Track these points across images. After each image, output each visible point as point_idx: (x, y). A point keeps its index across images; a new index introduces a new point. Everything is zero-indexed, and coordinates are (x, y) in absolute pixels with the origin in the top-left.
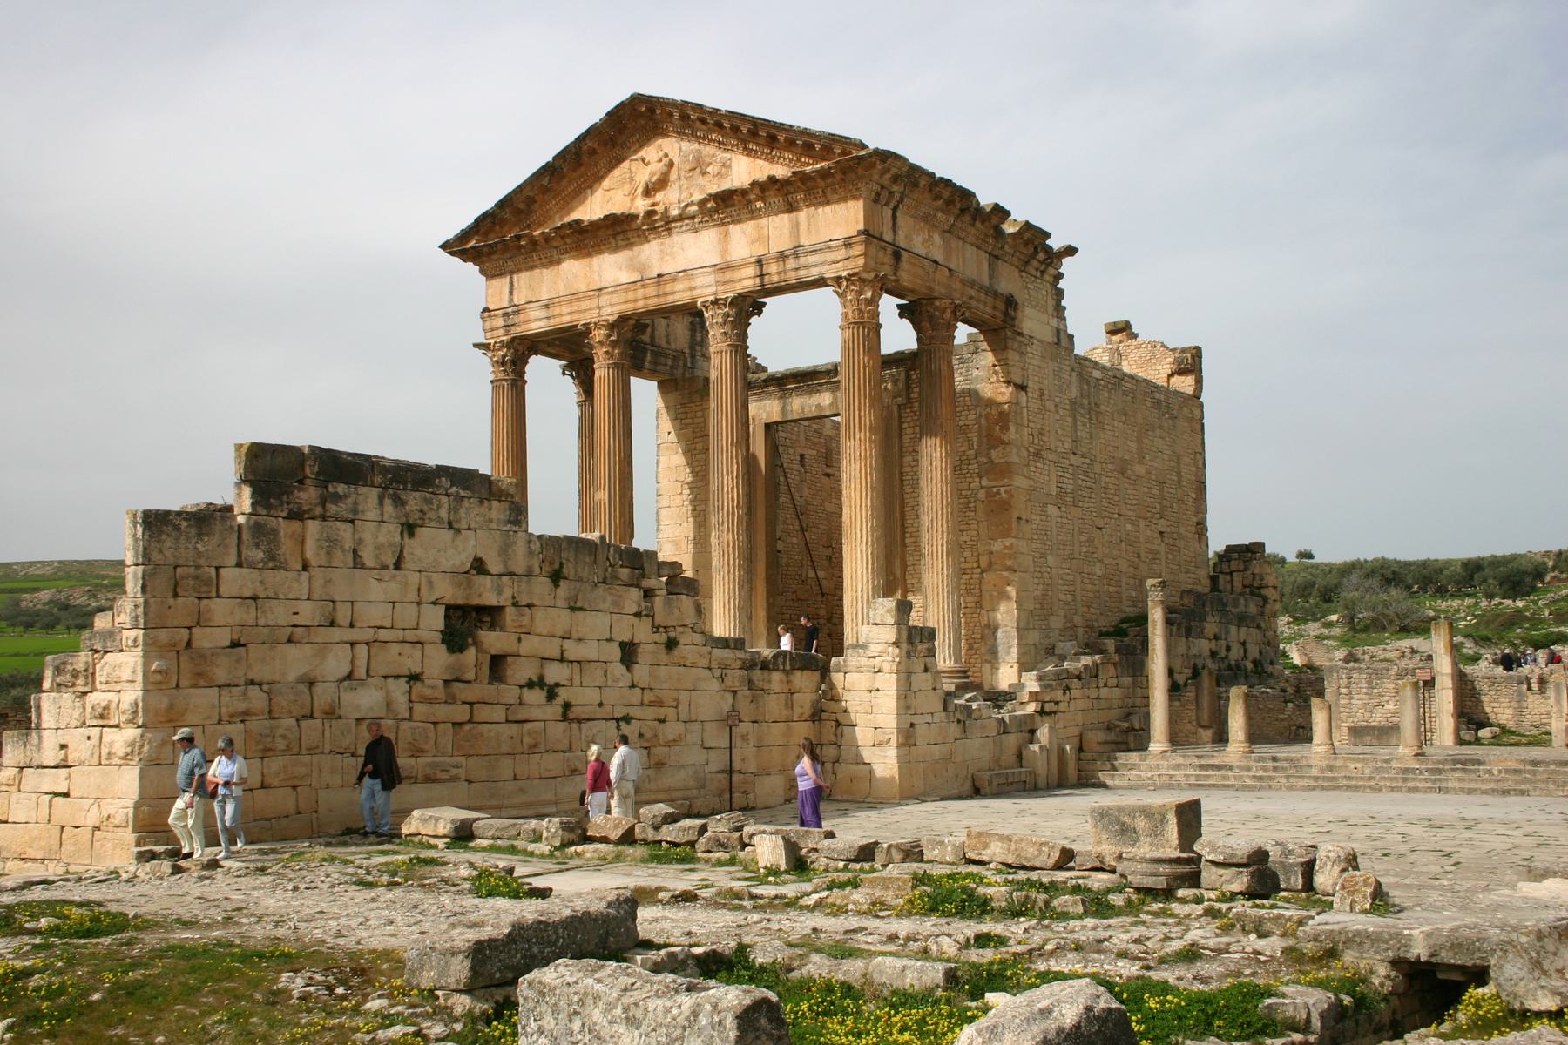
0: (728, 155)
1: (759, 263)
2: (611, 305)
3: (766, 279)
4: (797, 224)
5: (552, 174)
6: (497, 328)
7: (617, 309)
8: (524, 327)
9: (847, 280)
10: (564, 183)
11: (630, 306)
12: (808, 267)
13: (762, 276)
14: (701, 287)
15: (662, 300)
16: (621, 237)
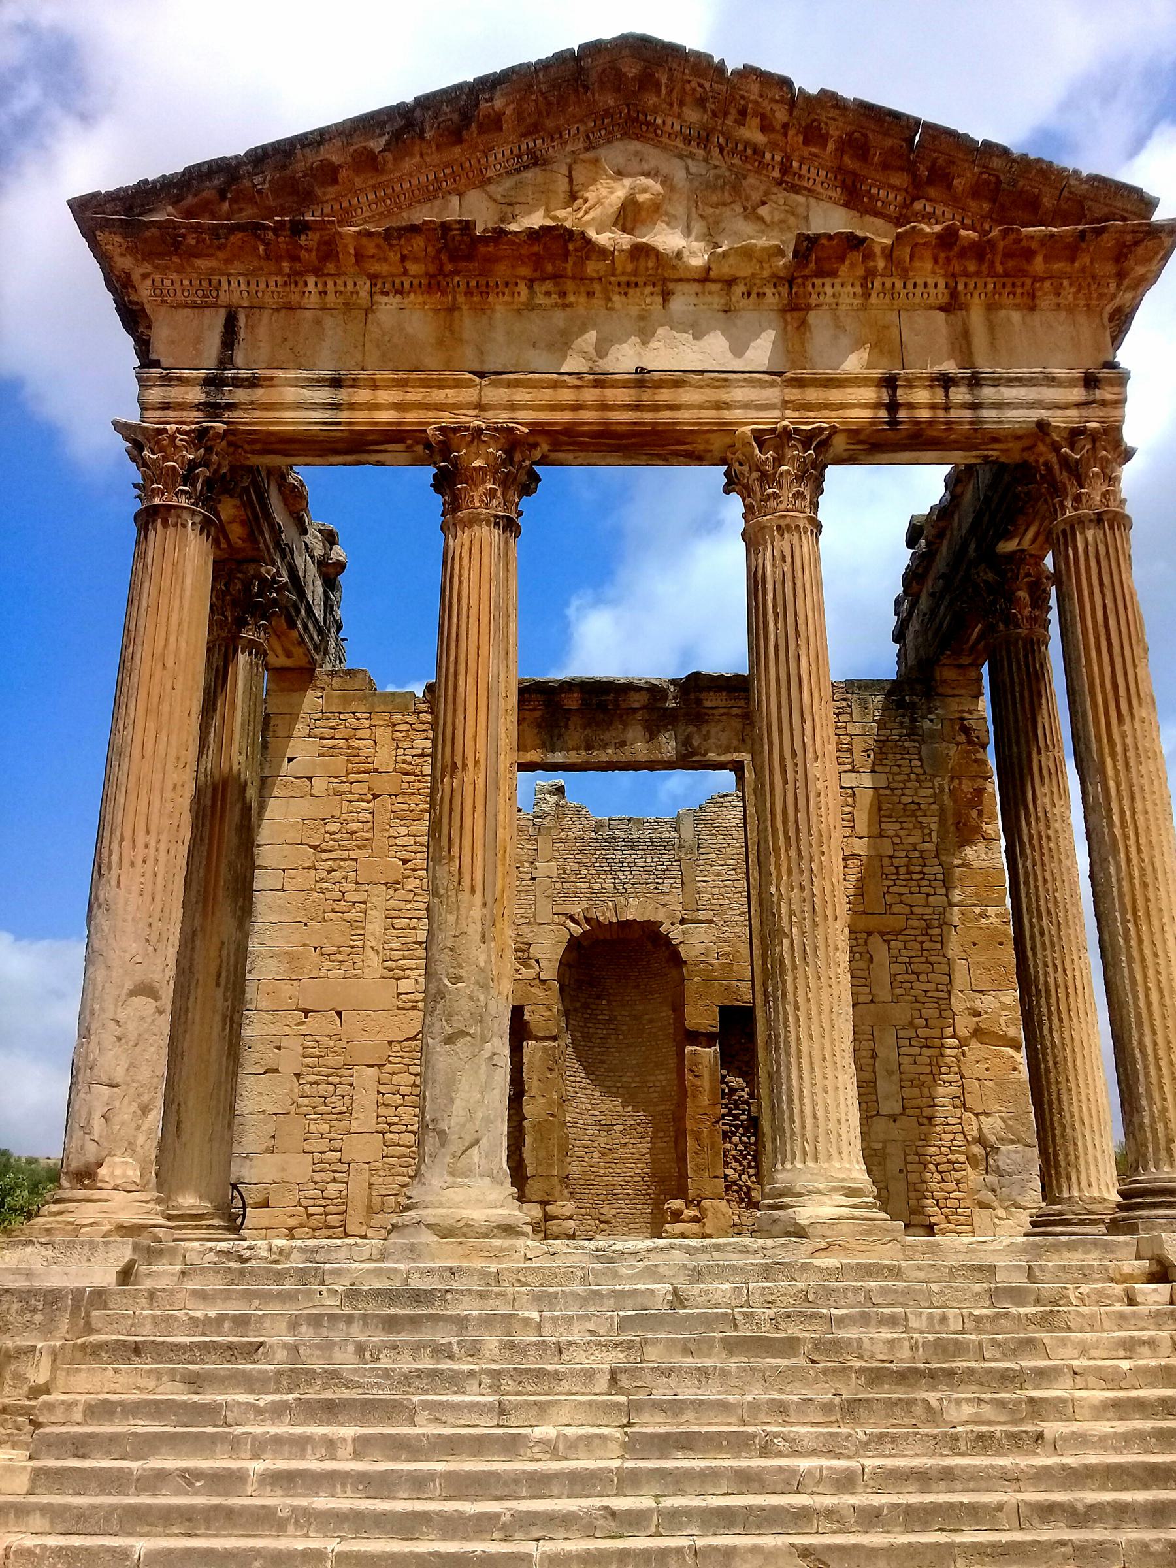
0: (801, 199)
1: (890, 382)
2: (512, 407)
3: (902, 415)
4: (966, 335)
5: (397, 136)
6: (181, 406)
7: (522, 415)
8: (258, 415)
9: (1094, 436)
10: (408, 164)
11: (567, 416)
12: (999, 405)
13: (893, 406)
14: (746, 406)
15: (647, 416)
16: (548, 285)
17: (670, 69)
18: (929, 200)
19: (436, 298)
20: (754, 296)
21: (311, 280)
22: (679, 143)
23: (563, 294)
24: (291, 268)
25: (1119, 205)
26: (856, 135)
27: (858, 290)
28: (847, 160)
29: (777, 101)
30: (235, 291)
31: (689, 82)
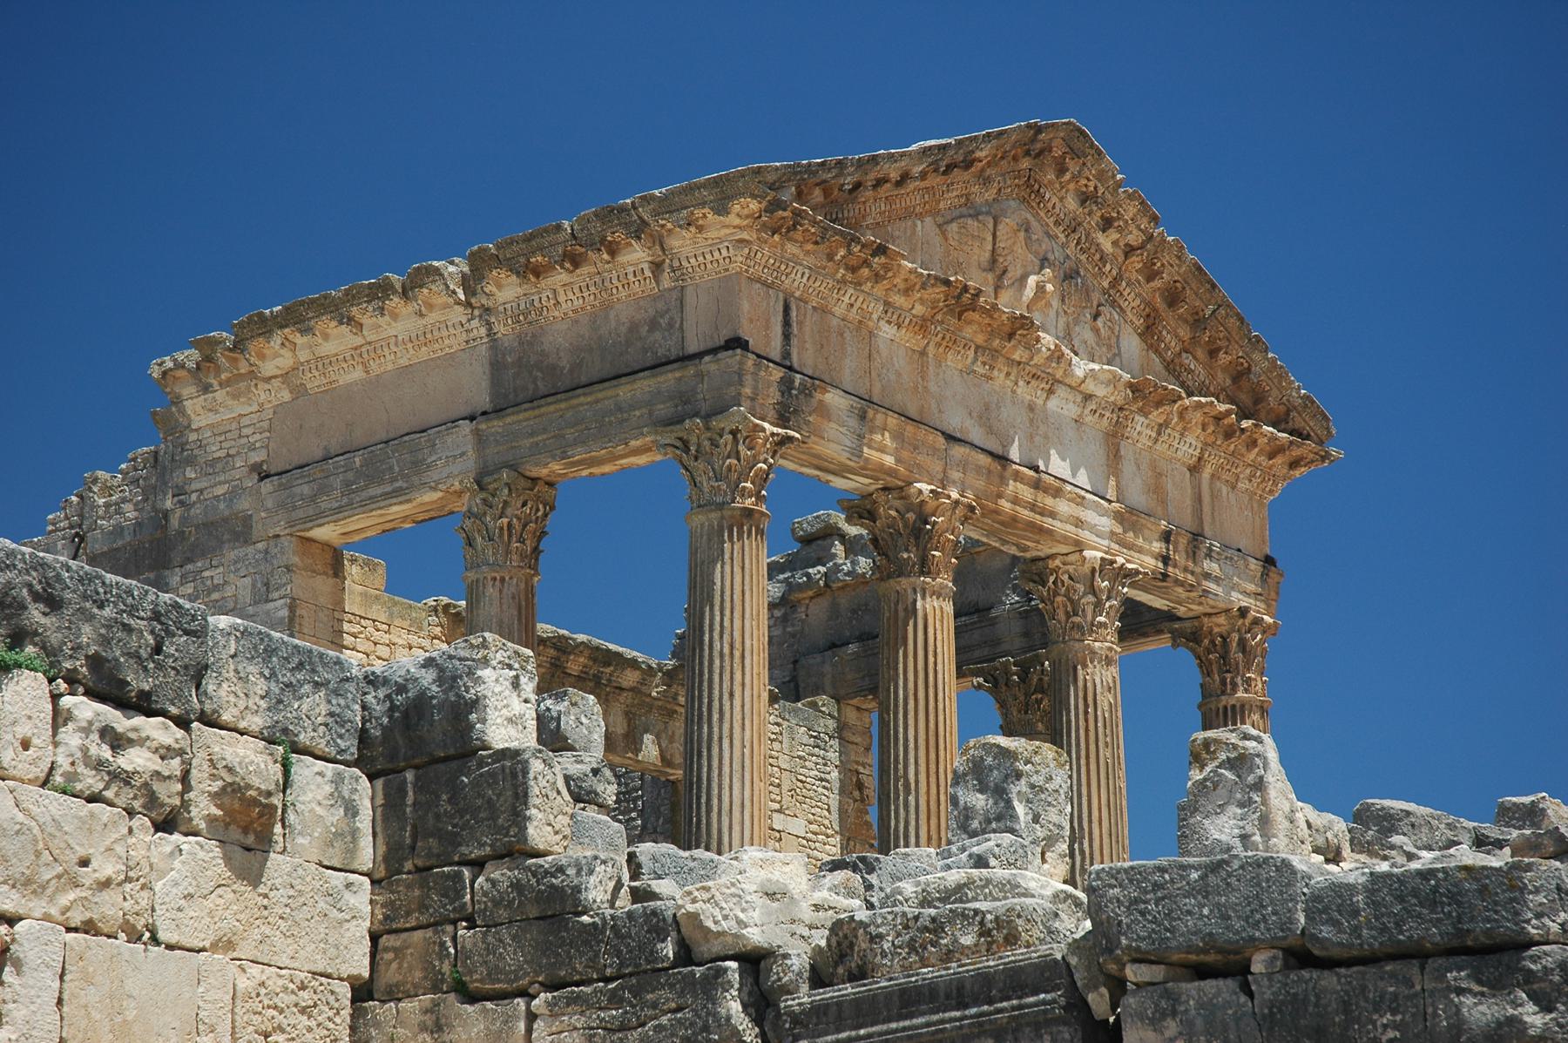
13: (1166, 560)
17: (1084, 164)
18: (1195, 358)
19: (917, 342)
20: (1097, 414)
21: (851, 291)
22: (1051, 221)
23: (992, 368)
24: (844, 275)
25: (1312, 424)
26: (1178, 285)
27: (1154, 435)
28: (1159, 302)
29: (1141, 230)
30: (797, 281)
31: (1089, 180)
